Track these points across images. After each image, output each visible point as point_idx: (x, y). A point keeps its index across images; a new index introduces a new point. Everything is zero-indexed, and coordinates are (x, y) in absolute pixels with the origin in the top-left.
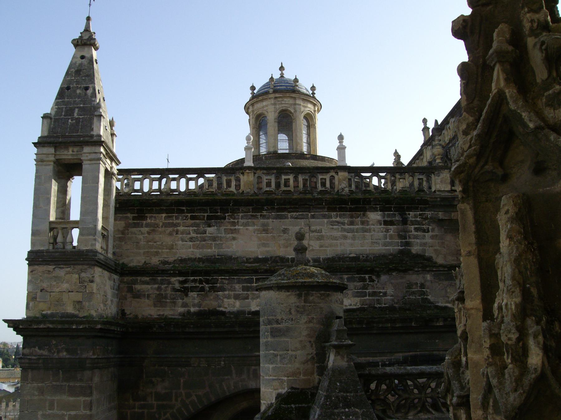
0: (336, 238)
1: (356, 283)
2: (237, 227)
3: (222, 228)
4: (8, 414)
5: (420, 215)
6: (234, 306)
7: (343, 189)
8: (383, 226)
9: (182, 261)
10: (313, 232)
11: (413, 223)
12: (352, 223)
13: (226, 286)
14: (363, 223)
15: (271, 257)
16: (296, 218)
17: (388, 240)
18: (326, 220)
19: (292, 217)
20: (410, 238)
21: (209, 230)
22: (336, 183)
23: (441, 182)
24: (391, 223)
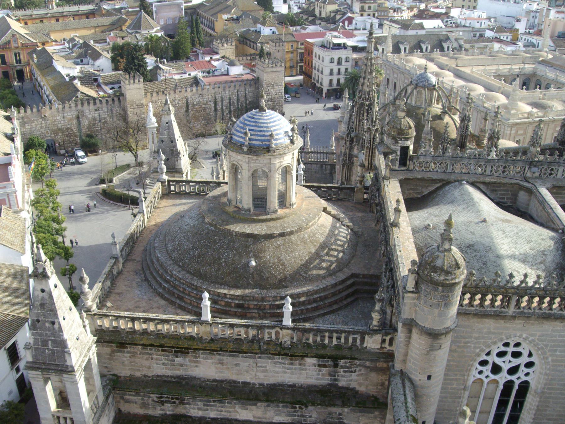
0: (277, 373)
1: (288, 409)
2: (198, 359)
3: (187, 359)
4: (65, 115)
5: (350, 362)
6: (198, 414)
7: (285, 342)
8: (317, 367)
9: (158, 376)
10: (259, 367)
11: (342, 367)
12: (291, 364)
13: (191, 402)
14: (300, 364)
15: (226, 380)
16: (246, 357)
17: (320, 376)
18: (270, 361)
19: (242, 357)
20: (338, 376)
21: (176, 359)
22: (281, 336)
23: (373, 342)
24: (325, 366)
